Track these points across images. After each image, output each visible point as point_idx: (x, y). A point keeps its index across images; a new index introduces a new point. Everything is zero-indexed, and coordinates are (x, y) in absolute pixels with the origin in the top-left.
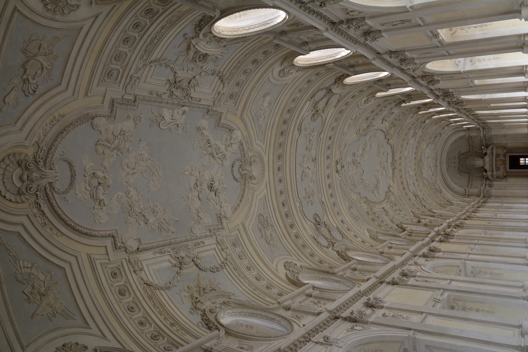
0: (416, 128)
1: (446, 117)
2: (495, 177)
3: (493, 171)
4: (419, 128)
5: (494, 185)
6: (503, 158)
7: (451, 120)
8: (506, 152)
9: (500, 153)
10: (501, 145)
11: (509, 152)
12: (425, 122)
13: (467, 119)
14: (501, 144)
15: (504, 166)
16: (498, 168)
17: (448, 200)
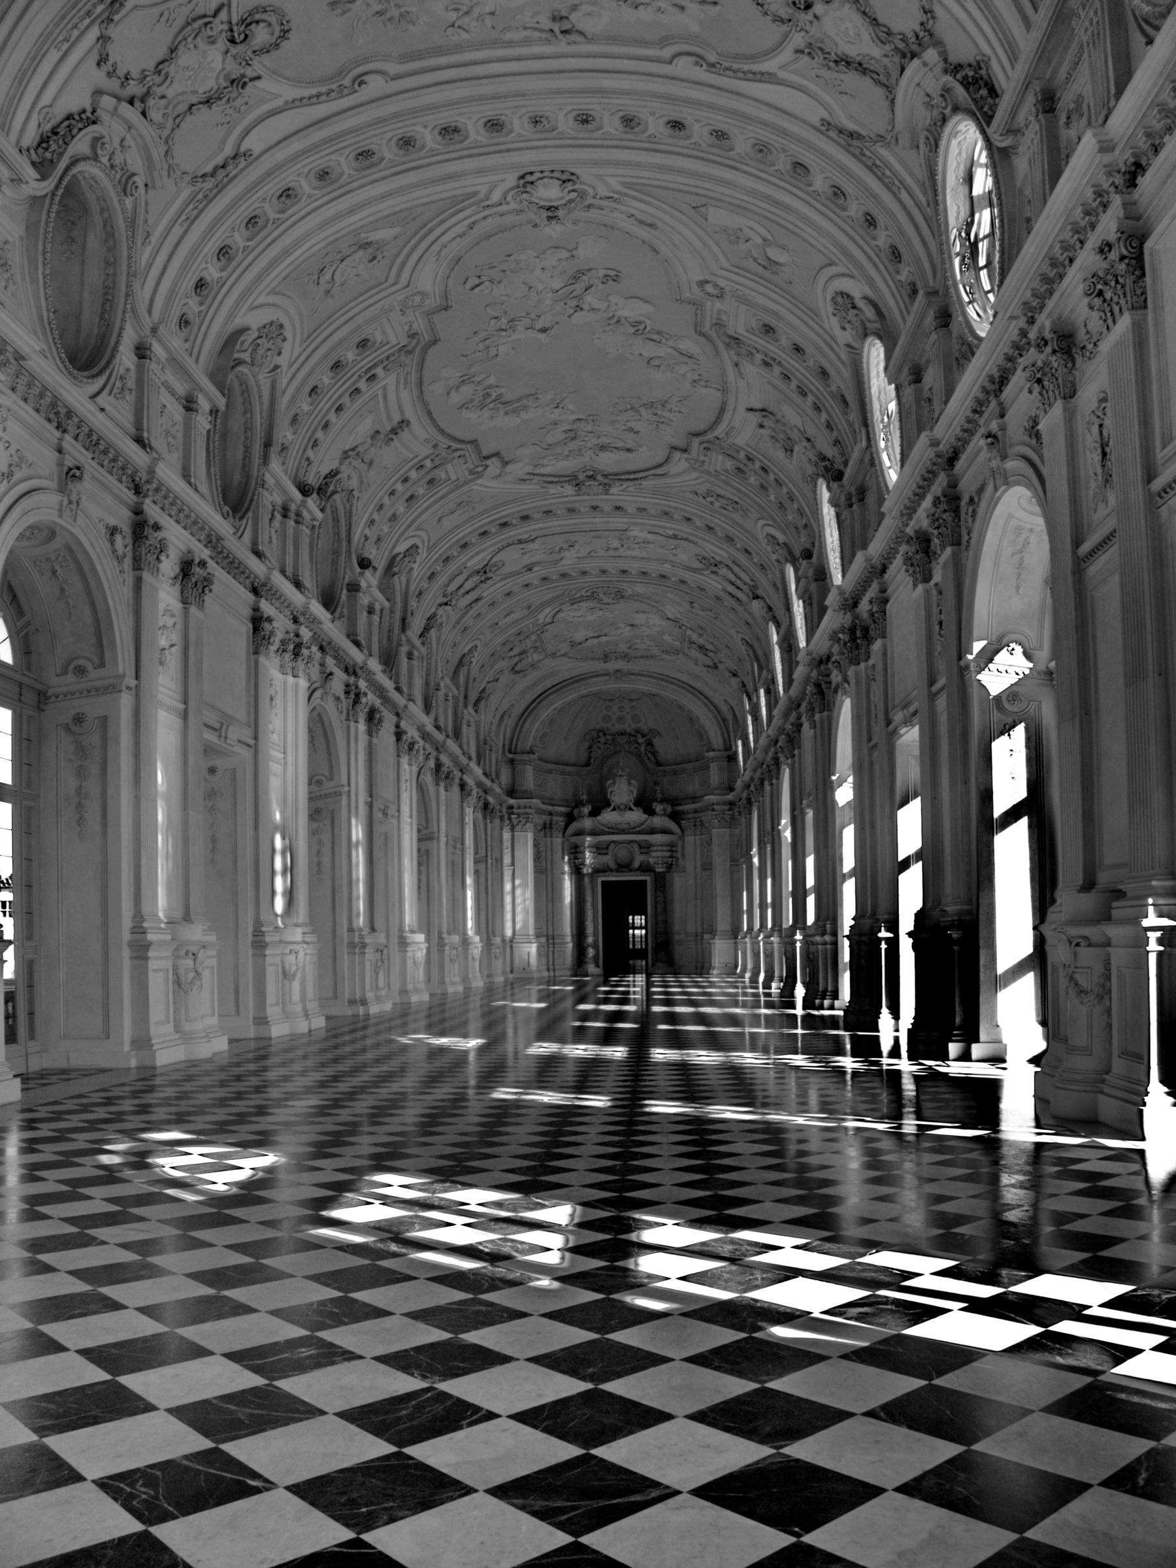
0: (736, 569)
1: (772, 672)
2: (575, 839)
3: (593, 833)
4: (733, 578)
5: (549, 839)
6: (636, 864)
7: (762, 692)
8: (658, 870)
9: (654, 854)
10: (679, 855)
11: (656, 880)
12: (756, 597)
13: (763, 741)
14: (683, 855)
15: (613, 865)
16: (607, 848)
17: (487, 692)
